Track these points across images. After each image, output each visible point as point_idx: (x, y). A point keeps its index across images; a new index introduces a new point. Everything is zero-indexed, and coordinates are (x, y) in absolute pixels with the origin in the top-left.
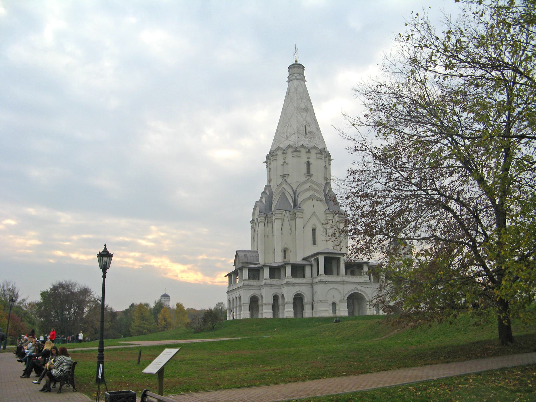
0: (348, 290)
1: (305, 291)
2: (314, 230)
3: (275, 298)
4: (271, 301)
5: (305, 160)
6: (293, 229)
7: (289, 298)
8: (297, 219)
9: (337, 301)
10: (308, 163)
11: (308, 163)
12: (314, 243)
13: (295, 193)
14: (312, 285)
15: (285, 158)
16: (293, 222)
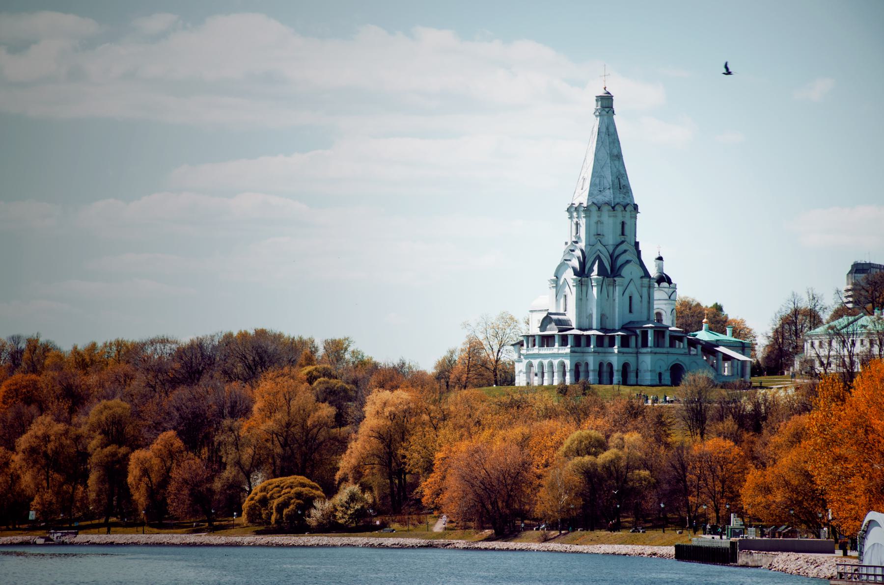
0: (672, 360)
1: (631, 359)
2: (630, 297)
3: (601, 365)
4: (597, 368)
5: (620, 219)
6: (611, 295)
7: (616, 366)
8: (617, 288)
9: (662, 371)
10: (623, 224)
11: (623, 224)
12: (630, 311)
13: (611, 256)
14: (637, 353)
15: (599, 217)
16: (611, 288)
